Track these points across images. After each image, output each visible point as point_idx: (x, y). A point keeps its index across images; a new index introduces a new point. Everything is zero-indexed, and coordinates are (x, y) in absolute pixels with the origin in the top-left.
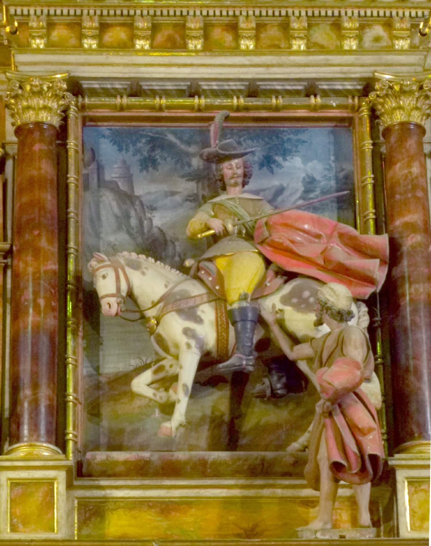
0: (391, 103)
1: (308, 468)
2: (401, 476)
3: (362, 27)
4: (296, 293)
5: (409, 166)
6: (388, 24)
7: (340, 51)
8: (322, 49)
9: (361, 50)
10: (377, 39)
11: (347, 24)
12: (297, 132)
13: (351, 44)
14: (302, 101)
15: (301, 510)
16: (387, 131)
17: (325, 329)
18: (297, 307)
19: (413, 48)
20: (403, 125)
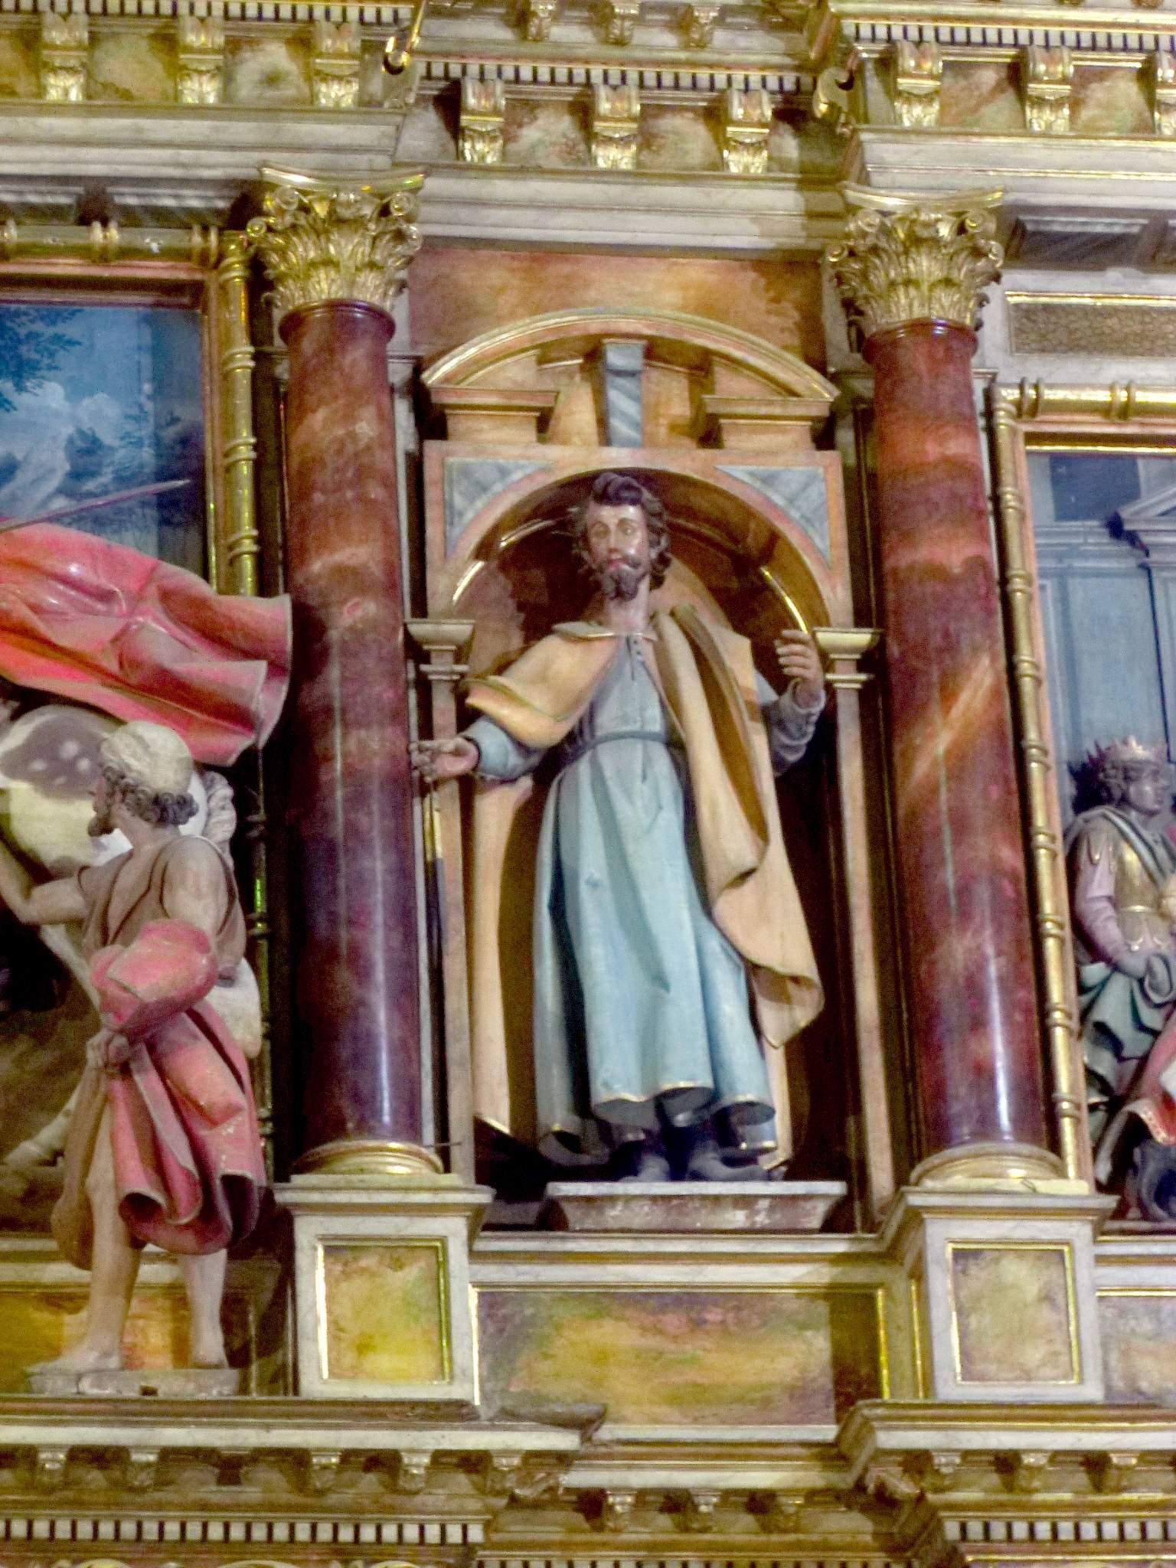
0: (304, 250)
1: (61, 1211)
2: (307, 1232)
3: (233, 46)
4: (42, 746)
5: (349, 417)
6: (303, 41)
7: (174, 107)
8: (125, 101)
9: (228, 107)
10: (272, 79)
11: (194, 38)
12: (53, 315)
13: (203, 89)
14: (73, 235)
15: (42, 1317)
16: (294, 323)
17: (118, 842)
18: (45, 783)
19: (366, 105)
20: (335, 306)
